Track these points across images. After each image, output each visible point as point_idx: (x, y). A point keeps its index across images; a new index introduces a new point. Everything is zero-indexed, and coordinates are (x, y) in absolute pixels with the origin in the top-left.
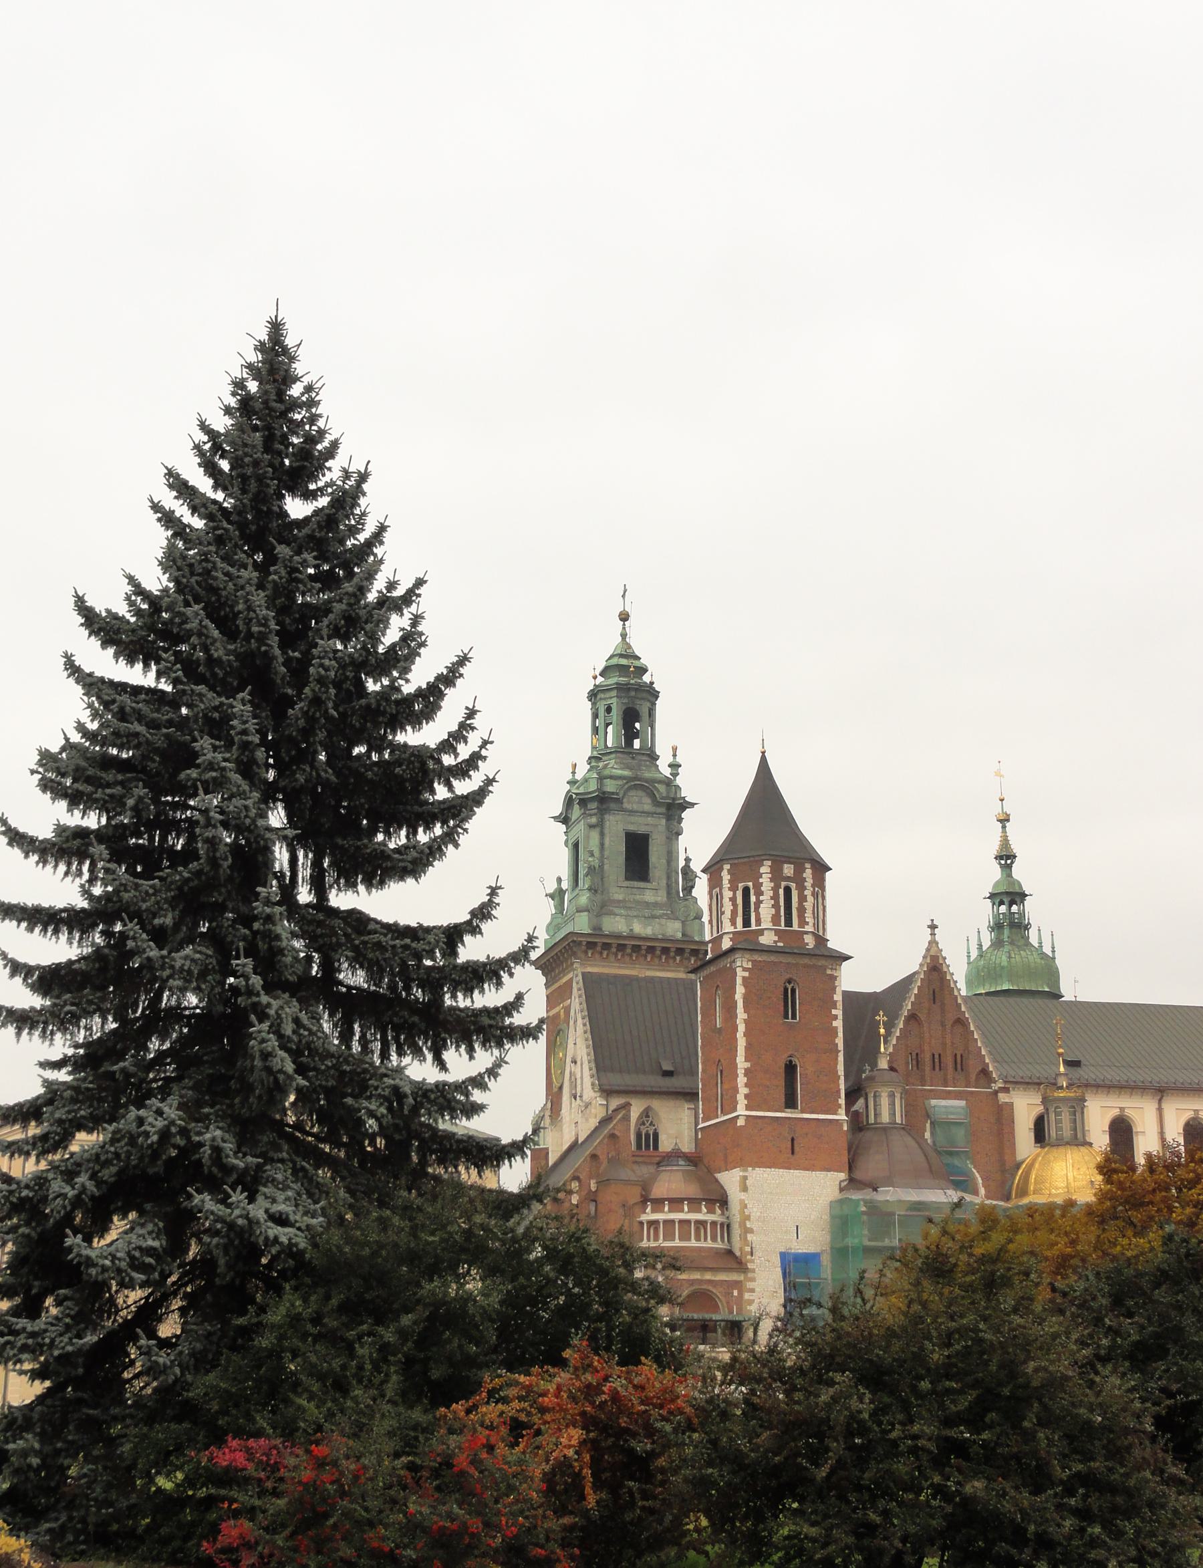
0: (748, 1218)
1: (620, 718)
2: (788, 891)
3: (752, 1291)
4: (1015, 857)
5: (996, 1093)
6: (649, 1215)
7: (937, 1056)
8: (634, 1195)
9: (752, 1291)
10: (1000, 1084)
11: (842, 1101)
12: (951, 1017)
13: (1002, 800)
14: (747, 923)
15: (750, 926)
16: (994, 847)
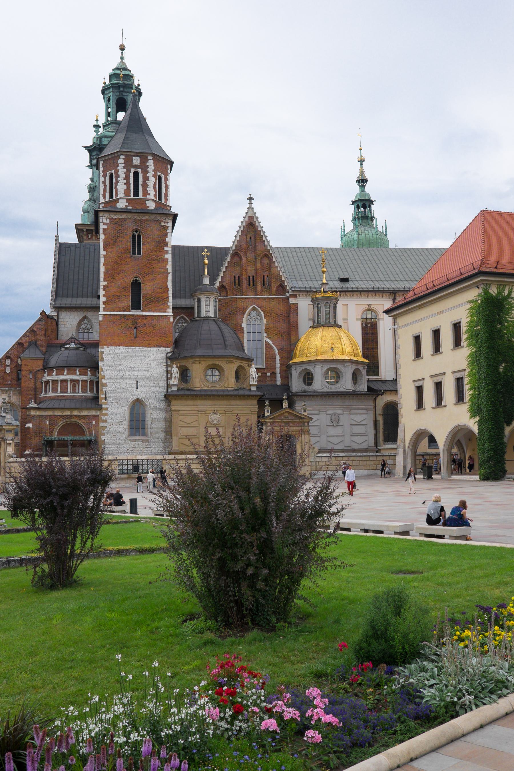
0: (104, 377)
1: (114, 103)
2: (136, 174)
3: (106, 421)
4: (366, 181)
5: (288, 298)
6: (46, 377)
7: (251, 278)
8: (40, 365)
9: (106, 421)
10: (290, 293)
11: (170, 304)
12: (260, 253)
13: (361, 149)
14: (111, 196)
15: (113, 198)
16: (356, 176)
